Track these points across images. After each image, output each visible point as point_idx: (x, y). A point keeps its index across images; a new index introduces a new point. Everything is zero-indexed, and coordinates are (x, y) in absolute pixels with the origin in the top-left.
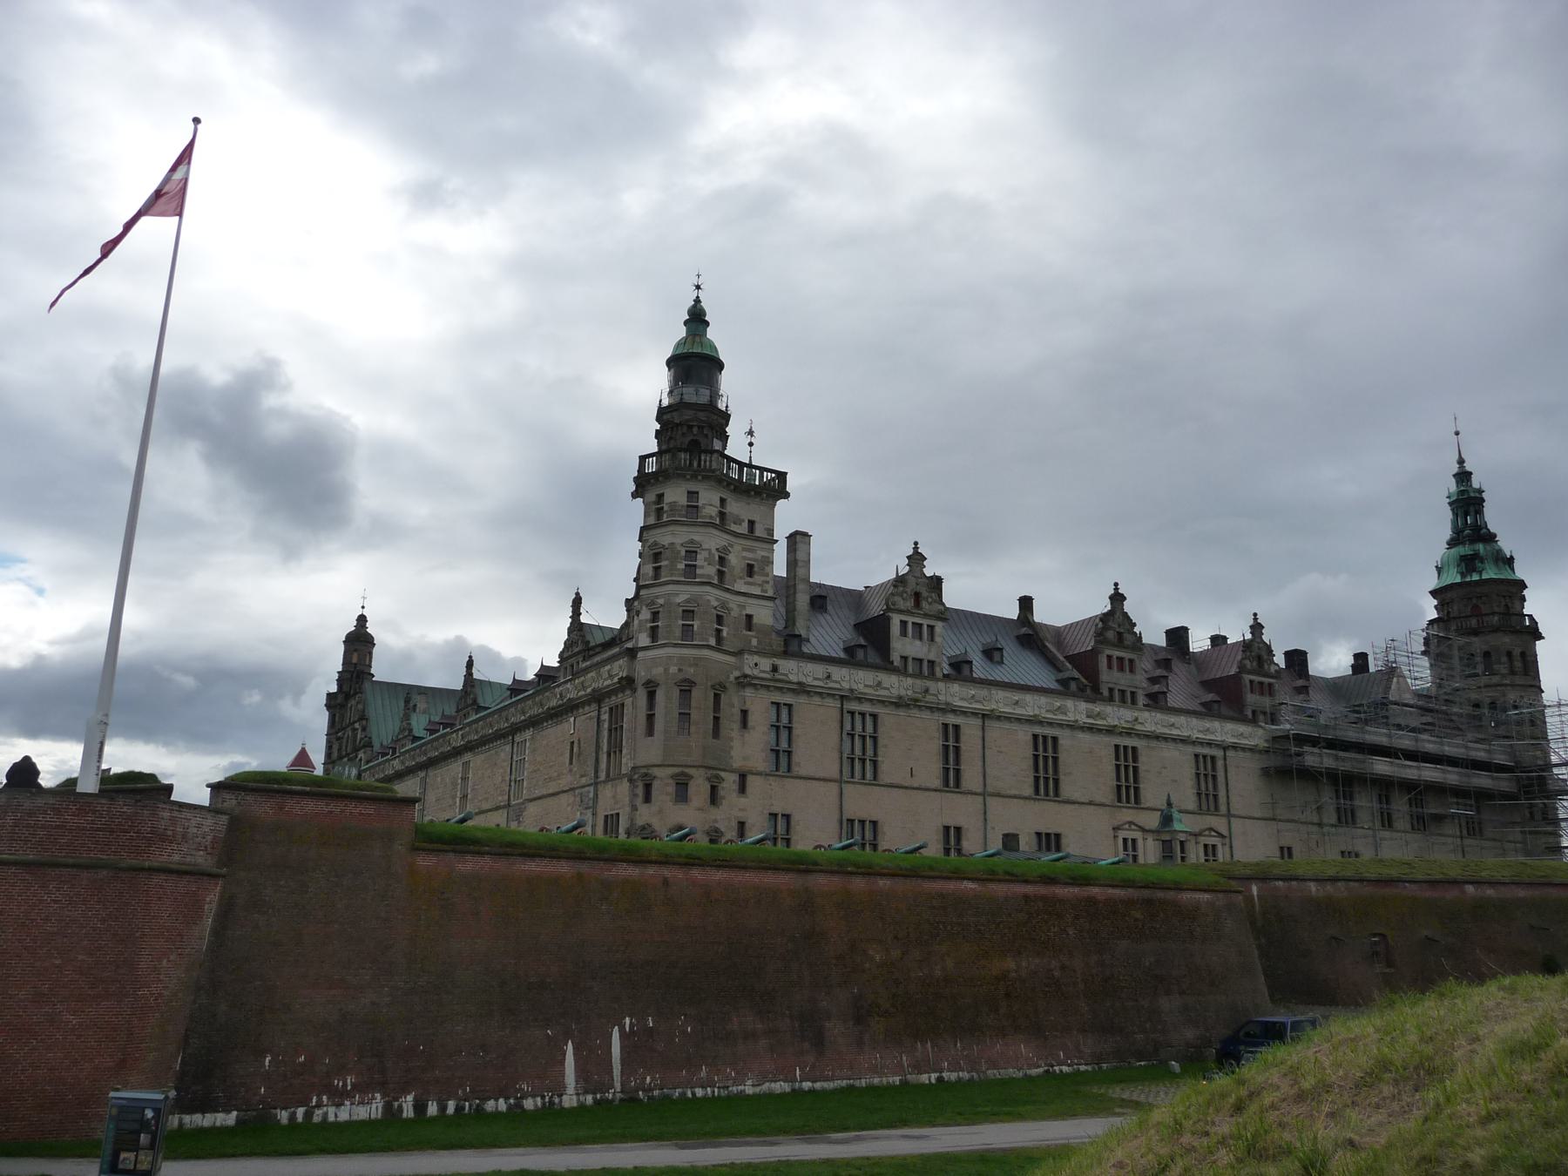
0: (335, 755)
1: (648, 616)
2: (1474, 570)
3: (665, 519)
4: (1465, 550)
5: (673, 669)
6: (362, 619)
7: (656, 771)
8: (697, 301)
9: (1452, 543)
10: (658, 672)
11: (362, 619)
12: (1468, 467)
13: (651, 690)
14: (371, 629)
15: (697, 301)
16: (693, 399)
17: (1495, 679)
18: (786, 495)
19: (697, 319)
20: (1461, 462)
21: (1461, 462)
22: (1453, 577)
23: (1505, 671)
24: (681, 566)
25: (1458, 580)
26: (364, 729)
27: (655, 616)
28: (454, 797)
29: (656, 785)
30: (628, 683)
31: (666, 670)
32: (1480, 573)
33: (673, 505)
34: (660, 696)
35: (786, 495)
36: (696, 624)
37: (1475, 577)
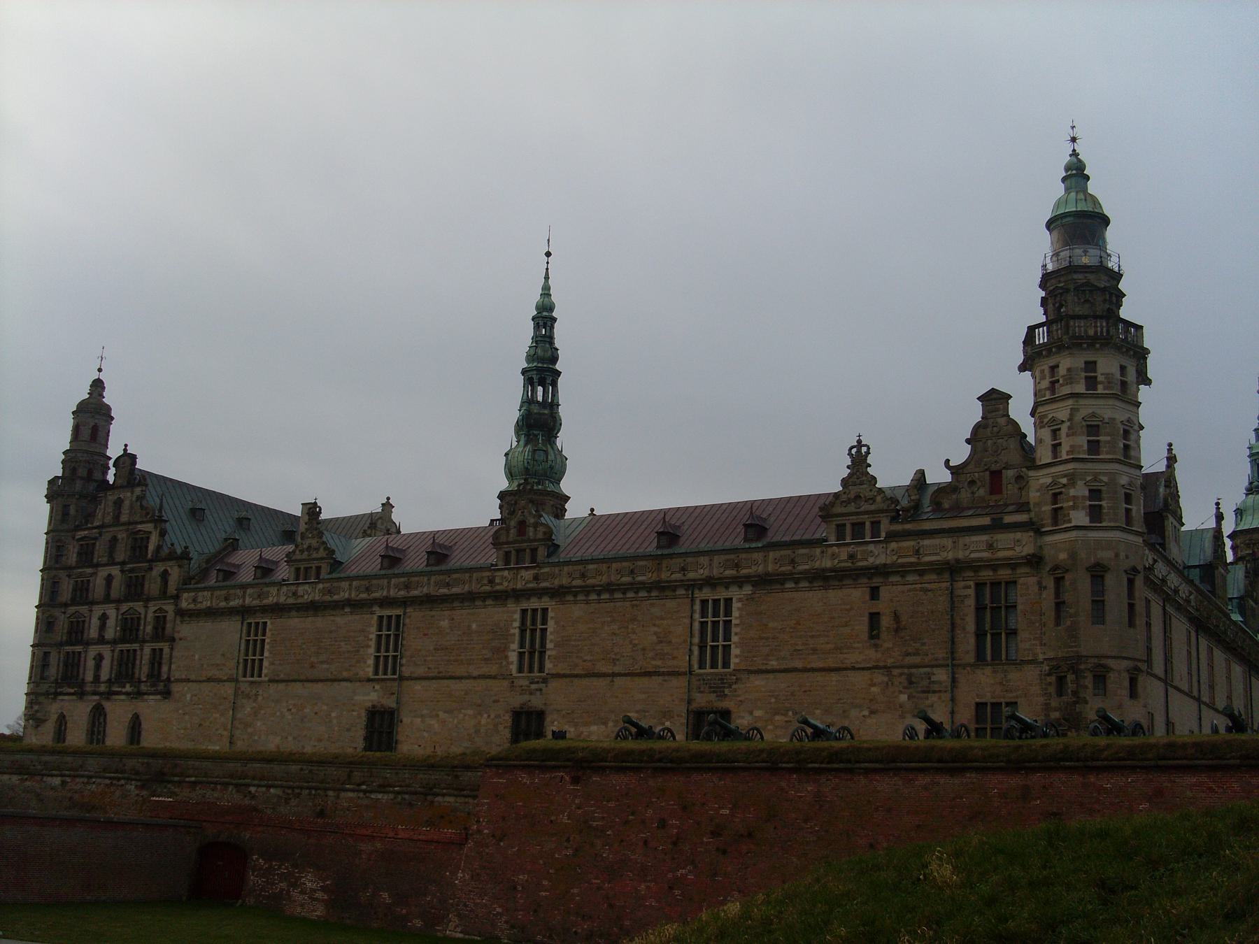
0: (72, 557)
1: (1087, 493)
3: (1100, 389)
6: (98, 385)
7: (1111, 663)
8: (1074, 154)
10: (1105, 555)
11: (98, 385)
13: (1098, 573)
14: (108, 399)
15: (1074, 154)
16: (1085, 260)
18: (1148, 382)
19: (1076, 174)
26: (163, 534)
27: (1095, 494)
28: (501, 651)
29: (1112, 676)
30: (1035, 561)
31: (1117, 555)
34: (1110, 580)
35: (1148, 382)
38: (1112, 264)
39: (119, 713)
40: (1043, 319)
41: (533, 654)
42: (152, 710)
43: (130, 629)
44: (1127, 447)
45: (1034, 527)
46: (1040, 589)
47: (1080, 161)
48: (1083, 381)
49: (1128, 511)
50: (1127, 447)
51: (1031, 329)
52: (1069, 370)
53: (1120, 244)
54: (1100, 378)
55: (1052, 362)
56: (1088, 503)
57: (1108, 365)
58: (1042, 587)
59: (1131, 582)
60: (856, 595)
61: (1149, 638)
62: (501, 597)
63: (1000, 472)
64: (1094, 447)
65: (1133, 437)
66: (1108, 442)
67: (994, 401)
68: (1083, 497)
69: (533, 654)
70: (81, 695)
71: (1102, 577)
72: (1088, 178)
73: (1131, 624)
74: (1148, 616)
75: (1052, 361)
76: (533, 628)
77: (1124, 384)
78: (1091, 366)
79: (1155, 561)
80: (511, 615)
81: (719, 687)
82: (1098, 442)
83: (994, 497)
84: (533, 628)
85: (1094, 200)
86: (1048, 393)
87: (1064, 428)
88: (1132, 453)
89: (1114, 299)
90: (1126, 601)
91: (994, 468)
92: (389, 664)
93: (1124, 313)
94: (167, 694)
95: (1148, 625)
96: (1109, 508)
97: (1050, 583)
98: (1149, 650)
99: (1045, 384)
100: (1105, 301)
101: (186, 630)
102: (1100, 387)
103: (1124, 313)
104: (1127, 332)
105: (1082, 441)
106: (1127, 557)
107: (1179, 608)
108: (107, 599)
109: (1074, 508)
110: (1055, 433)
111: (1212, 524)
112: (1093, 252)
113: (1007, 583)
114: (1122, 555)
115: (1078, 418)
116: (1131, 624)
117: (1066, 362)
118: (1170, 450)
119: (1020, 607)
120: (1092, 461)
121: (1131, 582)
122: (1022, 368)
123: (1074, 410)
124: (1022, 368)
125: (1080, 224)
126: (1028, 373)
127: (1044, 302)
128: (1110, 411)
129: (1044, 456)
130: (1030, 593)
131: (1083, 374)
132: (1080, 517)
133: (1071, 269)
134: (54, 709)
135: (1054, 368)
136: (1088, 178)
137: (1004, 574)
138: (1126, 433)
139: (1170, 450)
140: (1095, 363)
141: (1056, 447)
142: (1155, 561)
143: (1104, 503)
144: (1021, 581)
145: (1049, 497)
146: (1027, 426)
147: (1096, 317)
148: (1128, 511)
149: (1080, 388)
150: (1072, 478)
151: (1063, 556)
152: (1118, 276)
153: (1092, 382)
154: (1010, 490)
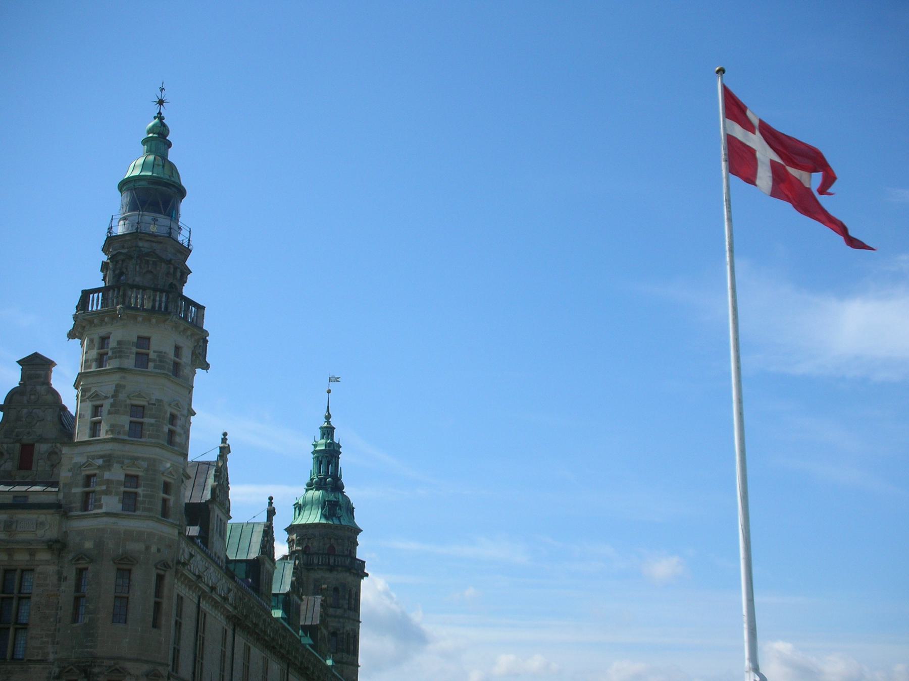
1: (122, 478)
2: (334, 515)
4: (332, 497)
5: (154, 549)
7: (129, 665)
9: (310, 486)
10: (134, 547)
12: (333, 424)
13: (125, 566)
15: (160, 117)
16: (153, 229)
17: (339, 612)
18: (206, 367)
19: (159, 140)
20: (328, 417)
21: (328, 417)
22: (313, 517)
23: (346, 606)
24: (166, 429)
25: (324, 521)
30: (58, 547)
31: (148, 548)
32: (339, 518)
33: (161, 356)
34: (138, 574)
35: (206, 367)
36: (172, 499)
37: (336, 522)
38: (182, 238)
40: (102, 284)
44: (171, 433)
45: (60, 509)
46: (59, 579)
47: (164, 125)
48: (133, 356)
49: (165, 501)
50: (171, 433)
51: (86, 294)
52: (120, 343)
53: (194, 219)
54: (152, 355)
55: (103, 331)
56: (122, 489)
57: (163, 340)
58: (61, 578)
59: (160, 578)
61: (178, 640)
63: (32, 445)
64: (137, 429)
65: (179, 423)
66: (152, 425)
67: (36, 367)
68: (118, 482)
71: (130, 571)
72: (169, 145)
73: (156, 624)
74: (179, 613)
75: (103, 331)
77: (177, 367)
78: (144, 341)
79: (191, 556)
82: (142, 423)
83: (23, 473)
85: (172, 167)
86: (94, 364)
87: (107, 405)
88: (177, 439)
89: (178, 274)
90: (152, 600)
91: (26, 440)
93: (188, 291)
95: (178, 625)
96: (145, 496)
97: (71, 574)
98: (176, 652)
99: (94, 353)
100: (168, 274)
102: (151, 365)
103: (188, 291)
104: (187, 310)
105: (125, 420)
106: (159, 550)
107: (216, 605)
109: (107, 492)
110: (96, 410)
111: (263, 518)
112: (163, 220)
113: (23, 571)
114: (154, 549)
115: (122, 396)
116: (156, 624)
117: (118, 333)
118: (224, 440)
119: (34, 599)
120: (132, 443)
121: (160, 578)
122: (71, 335)
123: (119, 388)
124: (71, 335)
125: (156, 194)
126: (77, 341)
127: (105, 267)
128: (154, 388)
129: (81, 433)
131: (134, 350)
132: (111, 503)
133: (135, 235)
135: (104, 340)
136: (169, 145)
137: (21, 558)
138: (173, 418)
139: (224, 440)
140: (149, 339)
141: (95, 427)
142: (191, 556)
143: (140, 491)
144: (39, 569)
145: (80, 479)
146: (70, 399)
147: (155, 290)
148: (165, 501)
149: (129, 363)
150: (108, 460)
151: (89, 545)
152: (186, 251)
153: (142, 360)
154: (40, 465)
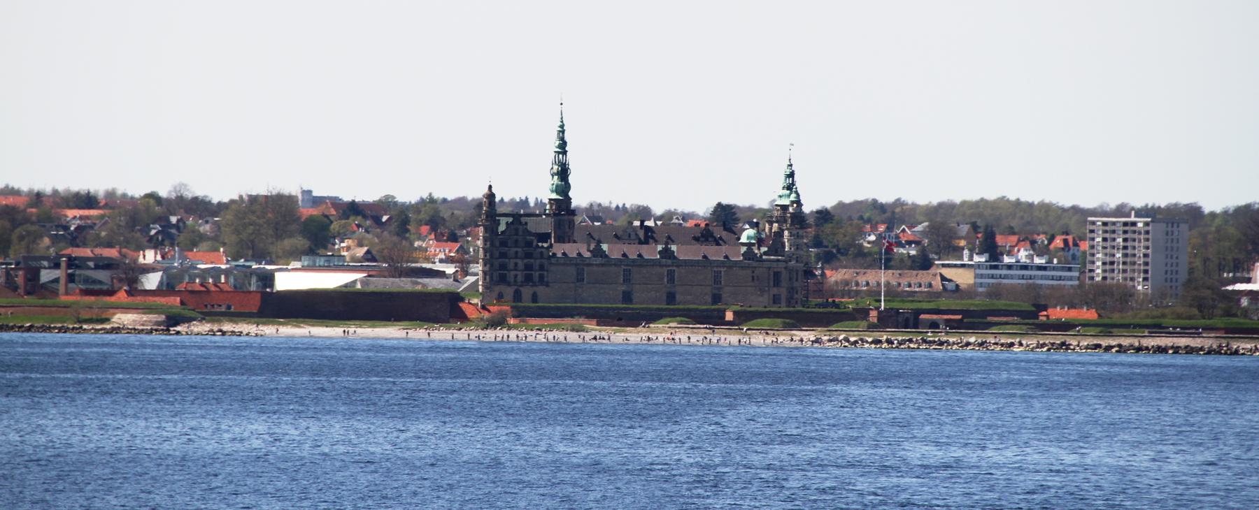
28: (662, 279)
39: (527, 292)
41: (671, 279)
42: (541, 290)
43: (528, 267)
60: (749, 271)
62: (661, 266)
69: (671, 279)
70: (509, 284)
76: (671, 275)
80: (665, 271)
81: (719, 289)
84: (671, 275)
92: (627, 280)
94: (547, 285)
101: (553, 268)
108: (516, 257)
130: (785, 275)
134: (497, 289)
